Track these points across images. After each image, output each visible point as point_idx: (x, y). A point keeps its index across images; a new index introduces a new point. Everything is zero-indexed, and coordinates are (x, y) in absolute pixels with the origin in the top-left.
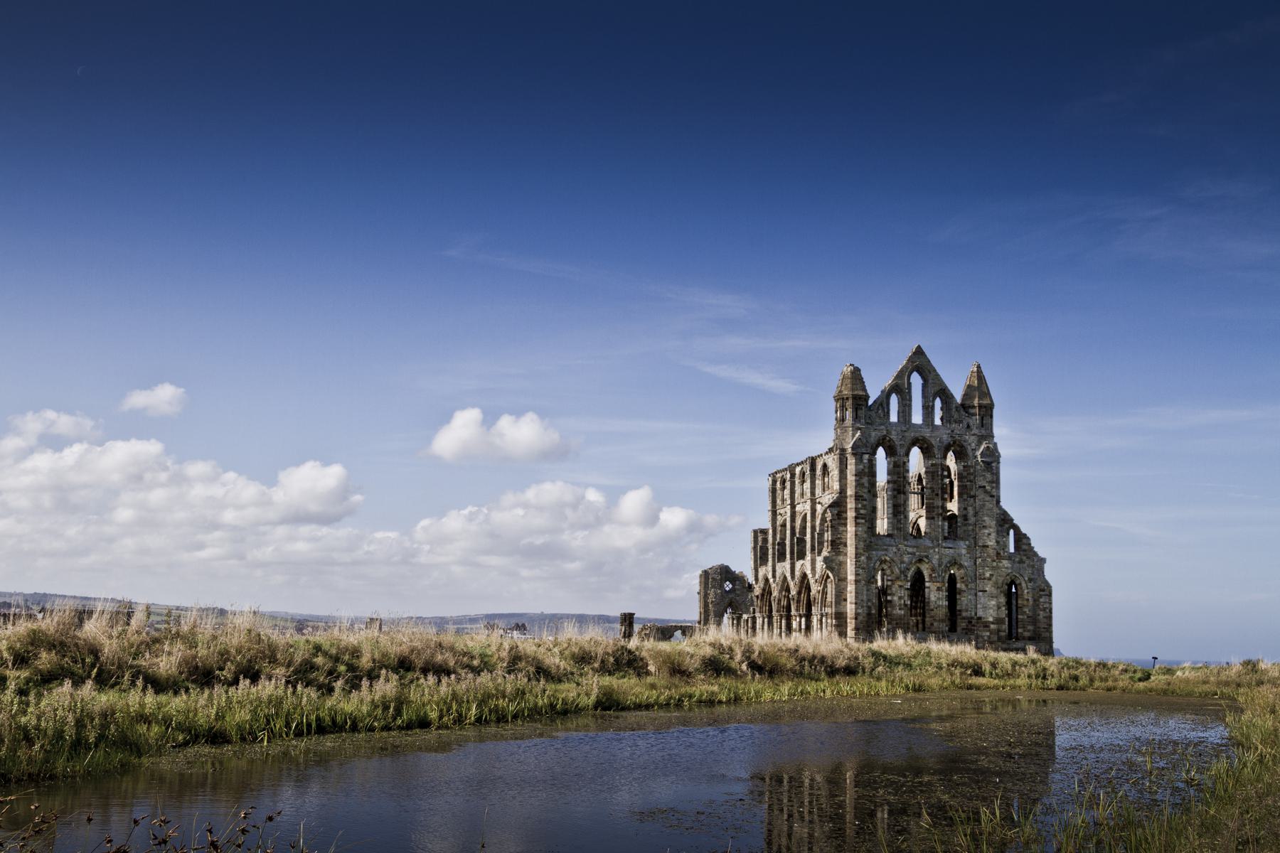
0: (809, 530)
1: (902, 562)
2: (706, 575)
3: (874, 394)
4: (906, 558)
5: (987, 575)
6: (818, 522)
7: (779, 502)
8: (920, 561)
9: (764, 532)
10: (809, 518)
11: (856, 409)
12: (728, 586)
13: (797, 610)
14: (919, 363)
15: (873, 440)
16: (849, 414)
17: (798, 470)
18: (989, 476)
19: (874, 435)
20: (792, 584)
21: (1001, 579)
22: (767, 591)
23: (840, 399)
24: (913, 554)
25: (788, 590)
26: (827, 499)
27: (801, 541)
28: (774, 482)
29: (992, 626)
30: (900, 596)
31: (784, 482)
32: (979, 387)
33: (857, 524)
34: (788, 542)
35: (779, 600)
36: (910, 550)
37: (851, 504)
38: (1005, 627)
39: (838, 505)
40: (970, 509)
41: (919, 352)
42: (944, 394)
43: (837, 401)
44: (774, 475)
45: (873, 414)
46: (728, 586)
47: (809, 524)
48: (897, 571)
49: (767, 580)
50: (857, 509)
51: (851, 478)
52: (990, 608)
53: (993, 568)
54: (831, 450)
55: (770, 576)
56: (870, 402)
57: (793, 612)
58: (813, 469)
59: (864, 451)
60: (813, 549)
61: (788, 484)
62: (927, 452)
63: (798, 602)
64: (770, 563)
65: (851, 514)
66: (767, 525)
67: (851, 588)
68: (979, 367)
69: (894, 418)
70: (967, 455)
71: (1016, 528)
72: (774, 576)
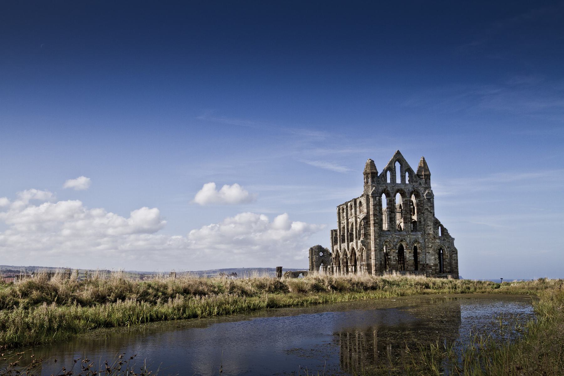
0: (354, 230)
1: (394, 242)
2: (312, 249)
3: (380, 172)
4: (396, 240)
5: (430, 246)
6: (358, 226)
7: (341, 218)
8: (402, 241)
9: (336, 231)
11: (373, 178)
12: (321, 254)
13: (351, 263)
14: (399, 157)
16: (370, 180)
17: (349, 204)
18: (429, 204)
19: (381, 189)
20: (348, 253)
21: (436, 248)
22: (338, 256)
23: (366, 174)
25: (346, 255)
26: (362, 216)
27: (351, 234)
28: (339, 210)
30: (393, 256)
31: (343, 209)
32: (424, 167)
33: (375, 226)
34: (346, 235)
36: (397, 236)
37: (372, 218)
38: (438, 267)
39: (366, 219)
40: (422, 218)
41: (398, 153)
42: (410, 170)
43: (364, 175)
44: (339, 207)
45: (380, 179)
46: (321, 254)
47: (354, 227)
49: (337, 251)
50: (374, 220)
51: (371, 207)
52: (431, 260)
53: (432, 243)
54: (363, 195)
55: (339, 249)
56: (379, 175)
57: (349, 264)
58: (355, 204)
59: (377, 195)
60: (356, 237)
61: (345, 210)
62: (403, 195)
63: (351, 260)
64: (339, 244)
65: (372, 222)
67: (373, 253)
68: (424, 158)
69: (389, 181)
70: (420, 196)
72: (340, 249)
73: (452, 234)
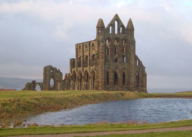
2: (45, 68)
6: (91, 58)
7: (78, 52)
8: (117, 68)
10: (88, 57)
15: (106, 38)
17: (85, 44)
19: (106, 37)
26: (94, 52)
28: (77, 46)
30: (111, 76)
31: (80, 46)
38: (136, 84)
41: (117, 16)
44: (77, 45)
48: (111, 70)
49: (74, 72)
52: (133, 80)
54: (95, 40)
66: (74, 57)
69: (111, 32)
71: (139, 60)
73: (144, 64)
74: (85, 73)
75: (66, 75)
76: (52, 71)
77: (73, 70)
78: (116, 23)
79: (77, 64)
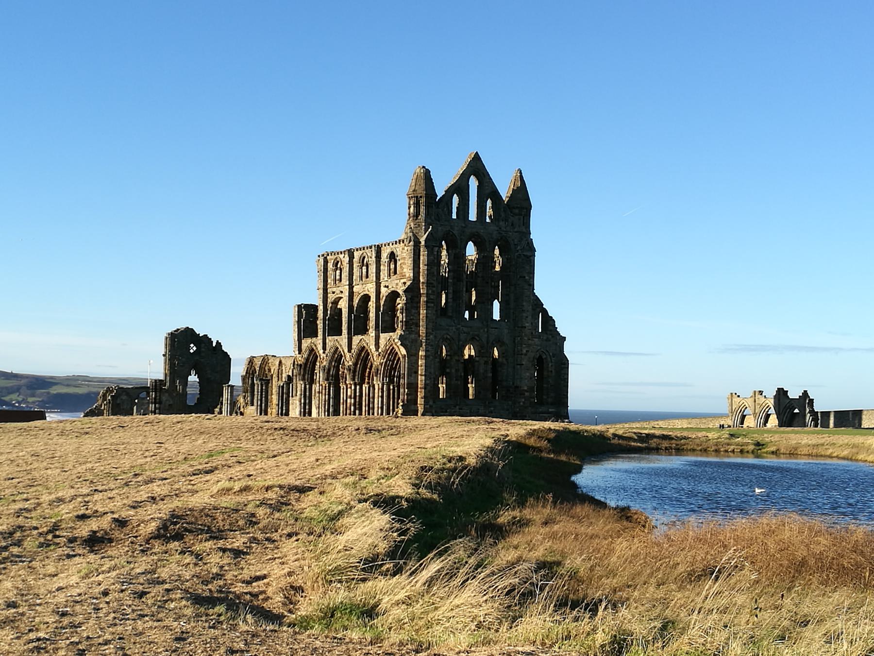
3: (440, 192)
4: (463, 336)
5: (524, 351)
9: (315, 308)
13: (353, 379)
14: (476, 167)
17: (357, 255)
24: (468, 333)
28: (326, 262)
29: (527, 394)
35: (329, 370)
36: (465, 329)
41: (477, 158)
46: (193, 348)
50: (428, 295)
52: (528, 377)
55: (320, 347)
63: (354, 372)
71: (545, 312)
72: (324, 348)
73: (562, 328)
74: (359, 355)
75: (251, 361)
76: (195, 348)
77: (306, 343)
78: (473, 183)
79: (324, 324)
